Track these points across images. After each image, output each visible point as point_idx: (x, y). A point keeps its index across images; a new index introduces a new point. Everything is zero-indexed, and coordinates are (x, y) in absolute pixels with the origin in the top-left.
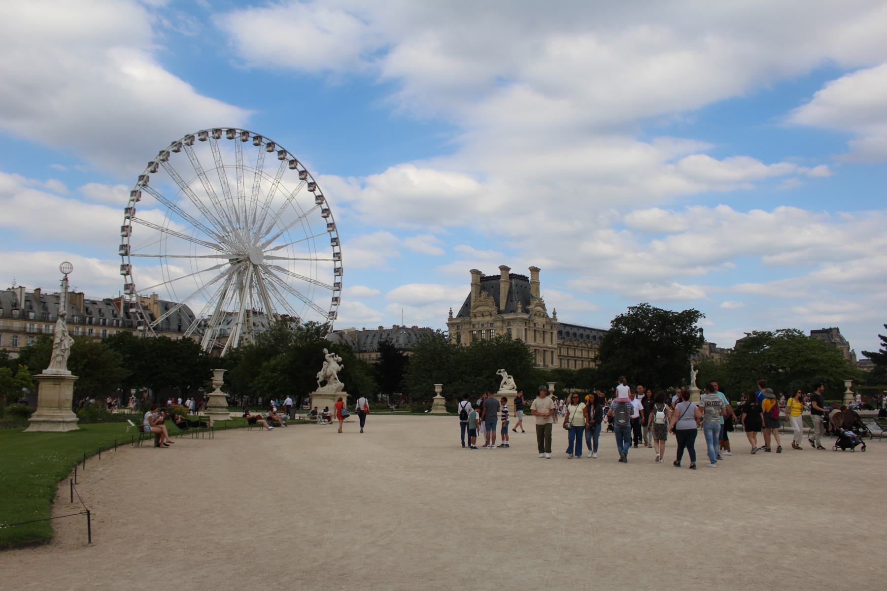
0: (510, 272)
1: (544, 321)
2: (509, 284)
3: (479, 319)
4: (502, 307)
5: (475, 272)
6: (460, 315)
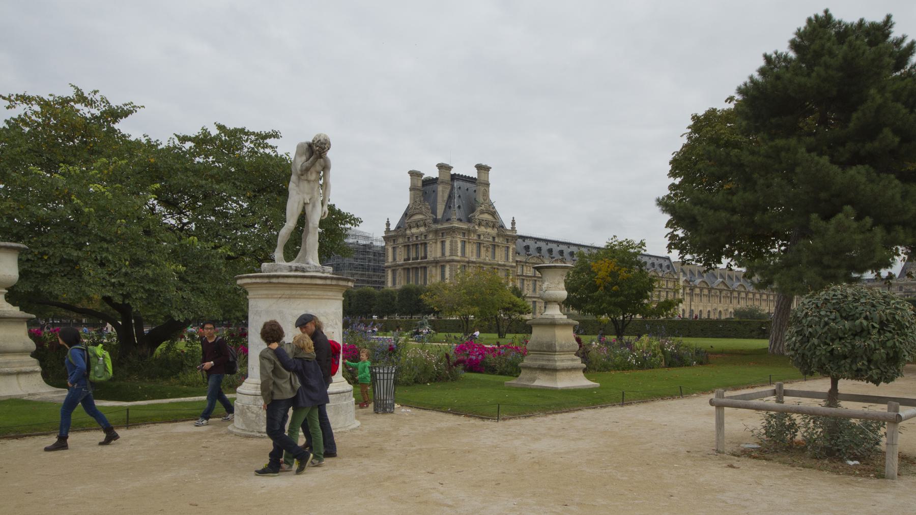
0: (452, 172)
1: (494, 232)
2: (449, 187)
3: (414, 230)
4: (439, 216)
5: (414, 174)
6: (398, 227)
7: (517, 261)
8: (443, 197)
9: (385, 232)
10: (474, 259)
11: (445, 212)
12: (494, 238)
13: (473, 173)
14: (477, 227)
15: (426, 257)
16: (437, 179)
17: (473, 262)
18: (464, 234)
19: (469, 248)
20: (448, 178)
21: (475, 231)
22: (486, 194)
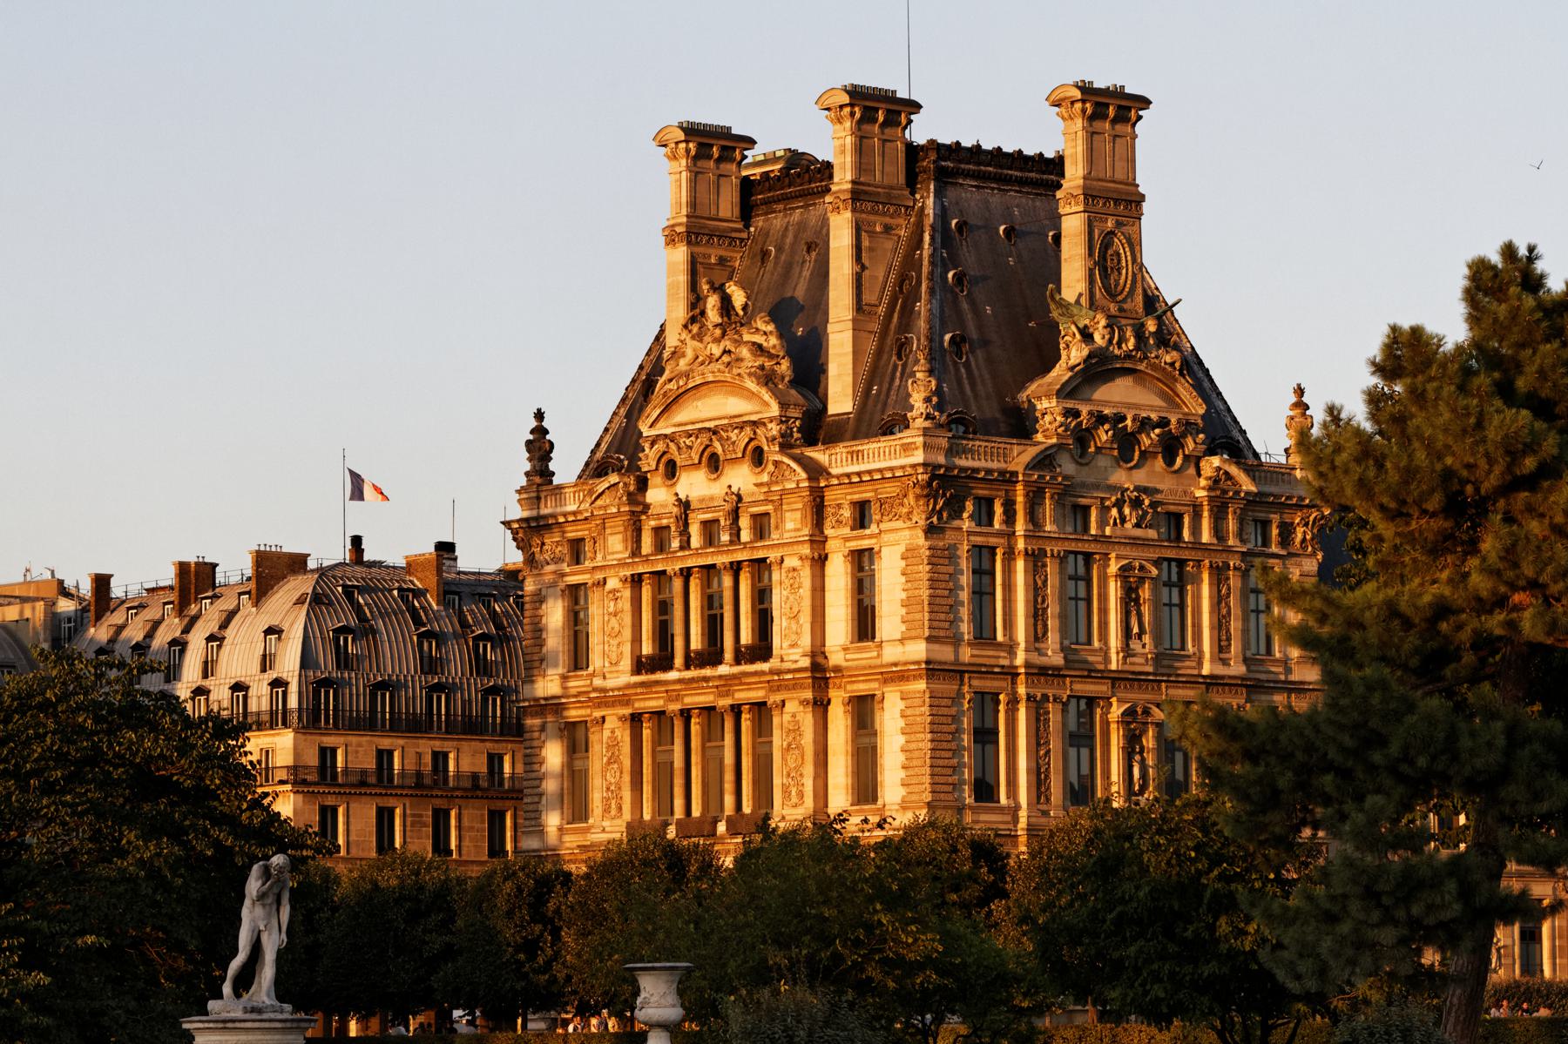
3: (695, 485)
4: (840, 399)
13: (1044, 133)
15: (762, 649)
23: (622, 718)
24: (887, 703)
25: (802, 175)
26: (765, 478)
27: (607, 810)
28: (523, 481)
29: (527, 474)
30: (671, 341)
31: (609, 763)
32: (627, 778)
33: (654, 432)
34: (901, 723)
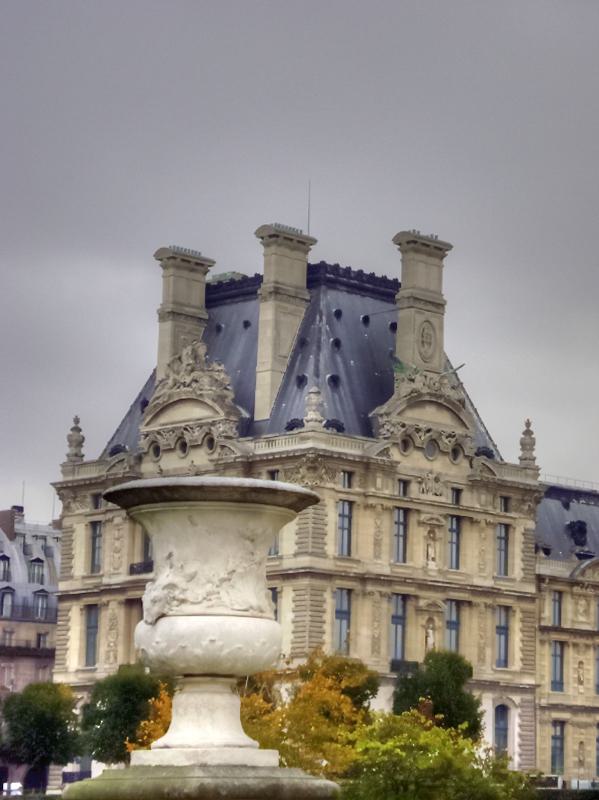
0: (314, 258)
1: (457, 472)
2: (302, 310)
4: (263, 410)
7: (540, 579)
8: (277, 345)
9: (66, 468)
10: (383, 566)
11: (282, 396)
12: (457, 492)
14: (395, 454)
16: (258, 279)
17: (378, 579)
18: (350, 475)
19: (366, 526)
20: (297, 278)
21: (390, 469)
22: (430, 337)
23: (120, 603)
24: (284, 594)
25: (243, 289)
26: (215, 456)
27: (108, 658)
28: (65, 459)
29: (68, 455)
30: (160, 376)
31: (111, 629)
32: (121, 638)
33: (148, 429)
34: (293, 605)
